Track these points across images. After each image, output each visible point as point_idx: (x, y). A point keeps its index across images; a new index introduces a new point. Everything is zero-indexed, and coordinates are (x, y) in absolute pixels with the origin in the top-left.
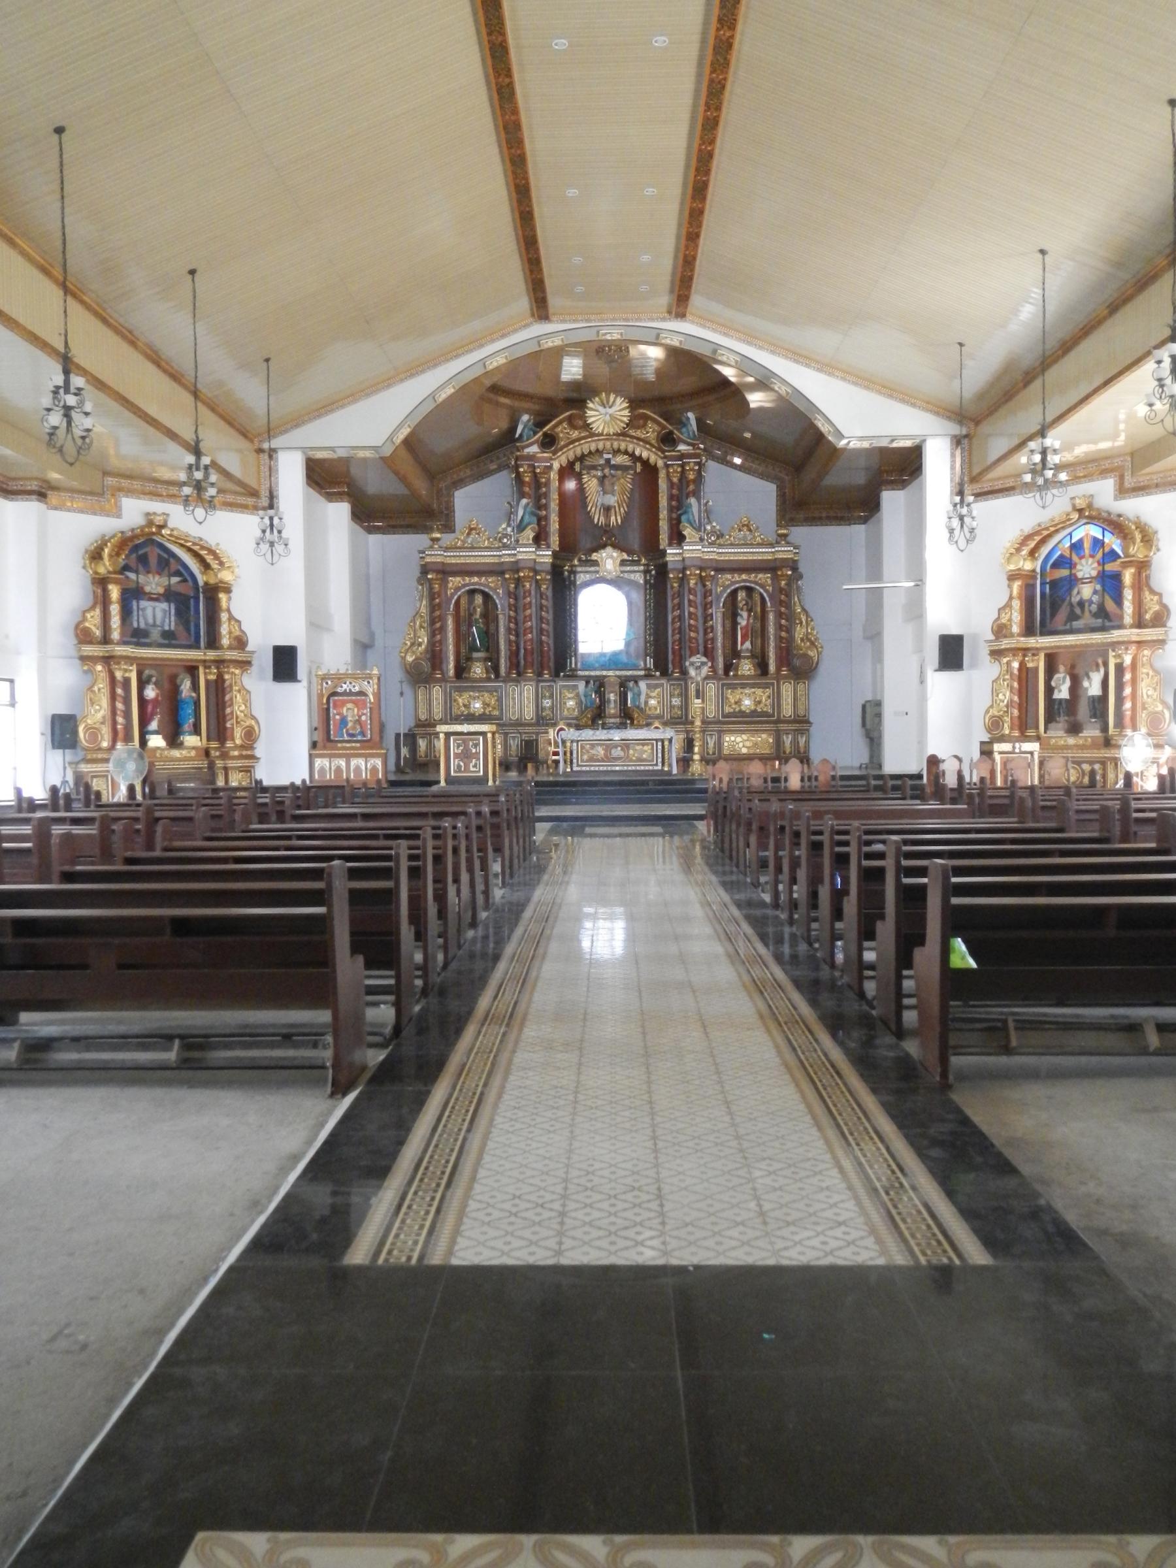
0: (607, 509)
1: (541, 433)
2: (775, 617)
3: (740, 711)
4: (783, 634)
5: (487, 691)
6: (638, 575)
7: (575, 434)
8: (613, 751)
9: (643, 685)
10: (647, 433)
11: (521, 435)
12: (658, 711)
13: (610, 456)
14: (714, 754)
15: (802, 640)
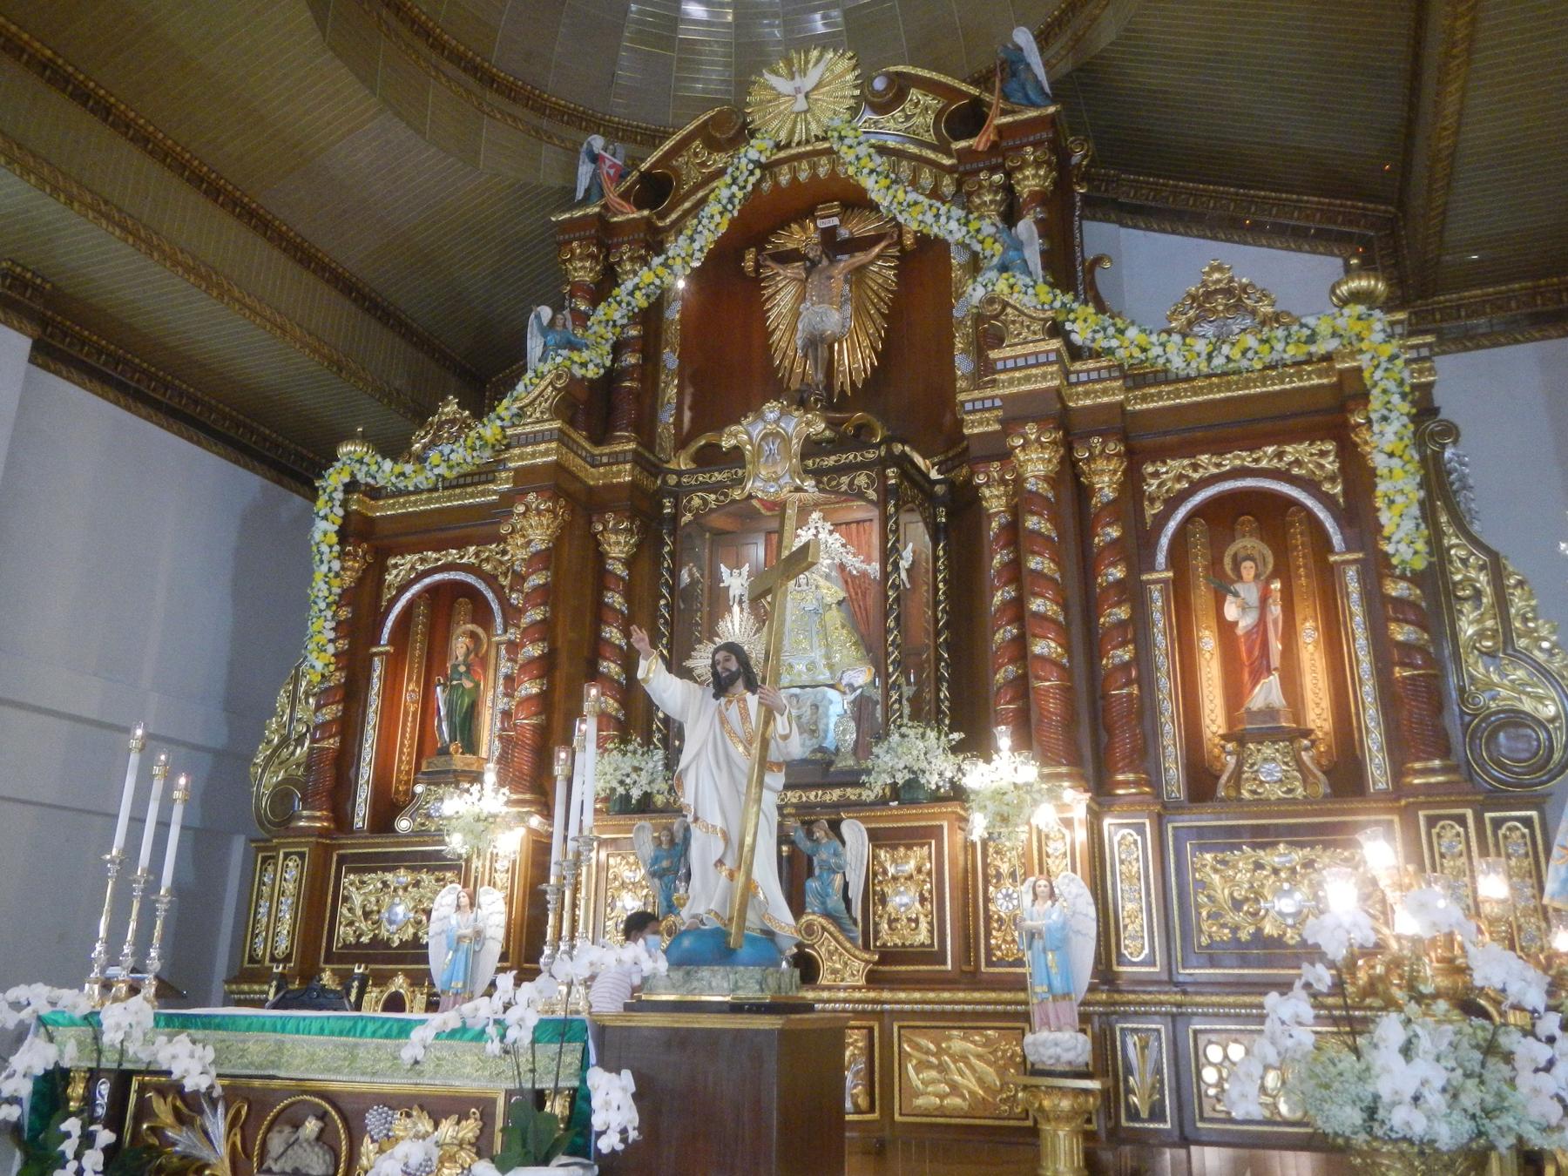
0: (818, 344)
1: (635, 174)
2: (1363, 577)
3: (1259, 938)
4: (1401, 633)
5: (431, 870)
6: (862, 480)
7: (719, 159)
8: (276, 1143)
9: (854, 831)
10: (908, 118)
11: (588, 191)
12: (922, 936)
13: (835, 221)
14: (1157, 1113)
15: (1490, 654)
